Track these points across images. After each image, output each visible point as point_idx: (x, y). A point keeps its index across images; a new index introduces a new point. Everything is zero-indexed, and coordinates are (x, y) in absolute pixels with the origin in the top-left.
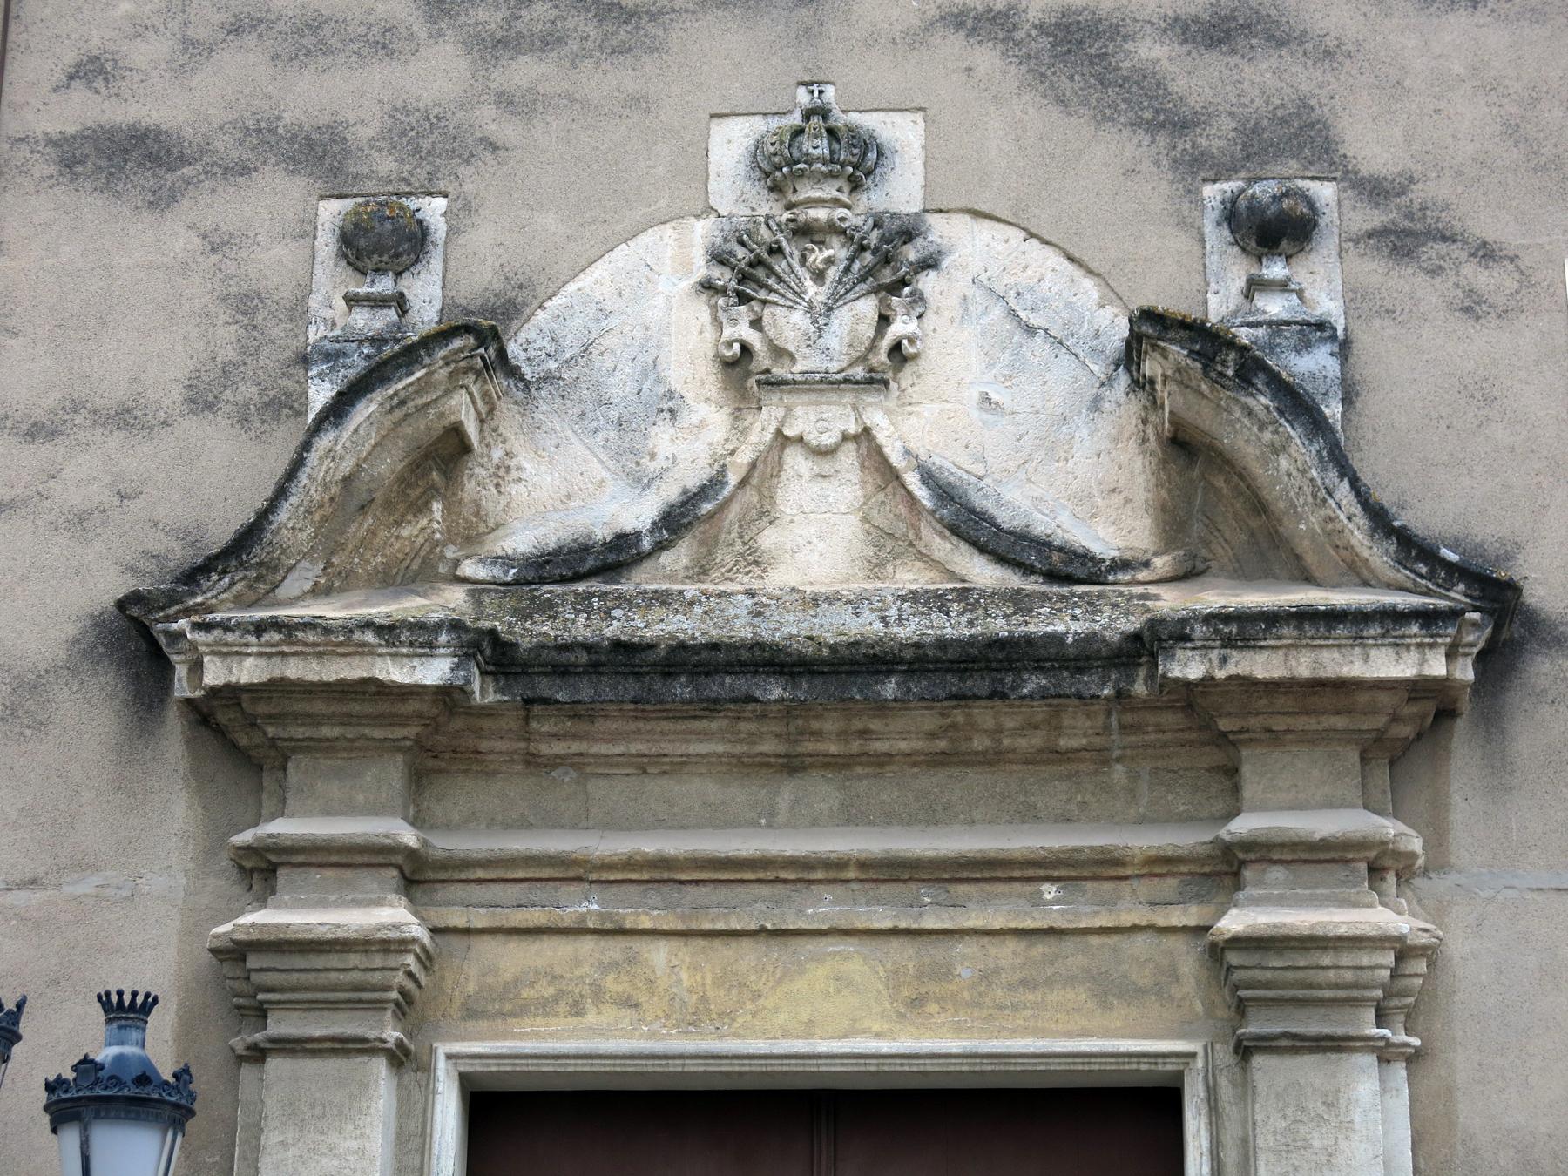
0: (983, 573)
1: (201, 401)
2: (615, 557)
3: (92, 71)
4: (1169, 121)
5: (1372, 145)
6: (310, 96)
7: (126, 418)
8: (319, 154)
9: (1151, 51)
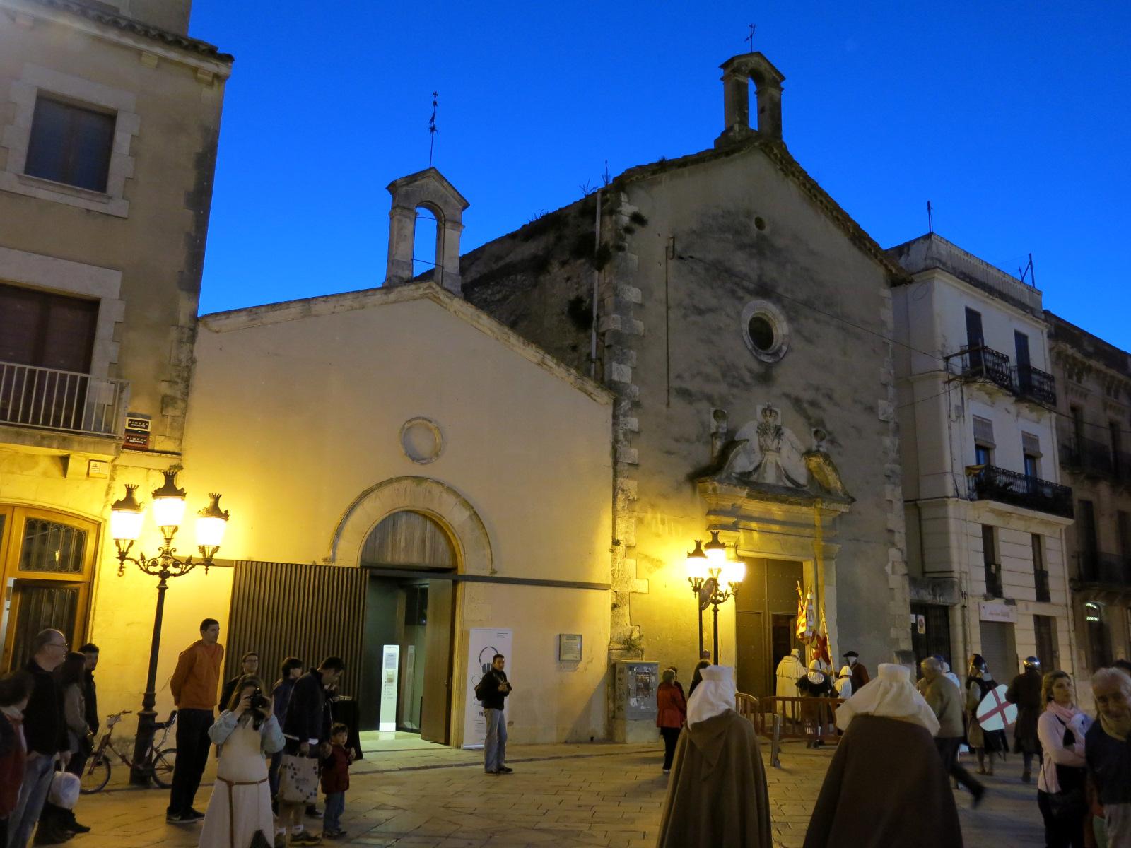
0: (789, 484)
1: (698, 439)
2: (750, 473)
3: (679, 377)
4: (808, 418)
5: (829, 426)
6: (709, 389)
7: (688, 440)
8: (710, 399)
9: (806, 405)
